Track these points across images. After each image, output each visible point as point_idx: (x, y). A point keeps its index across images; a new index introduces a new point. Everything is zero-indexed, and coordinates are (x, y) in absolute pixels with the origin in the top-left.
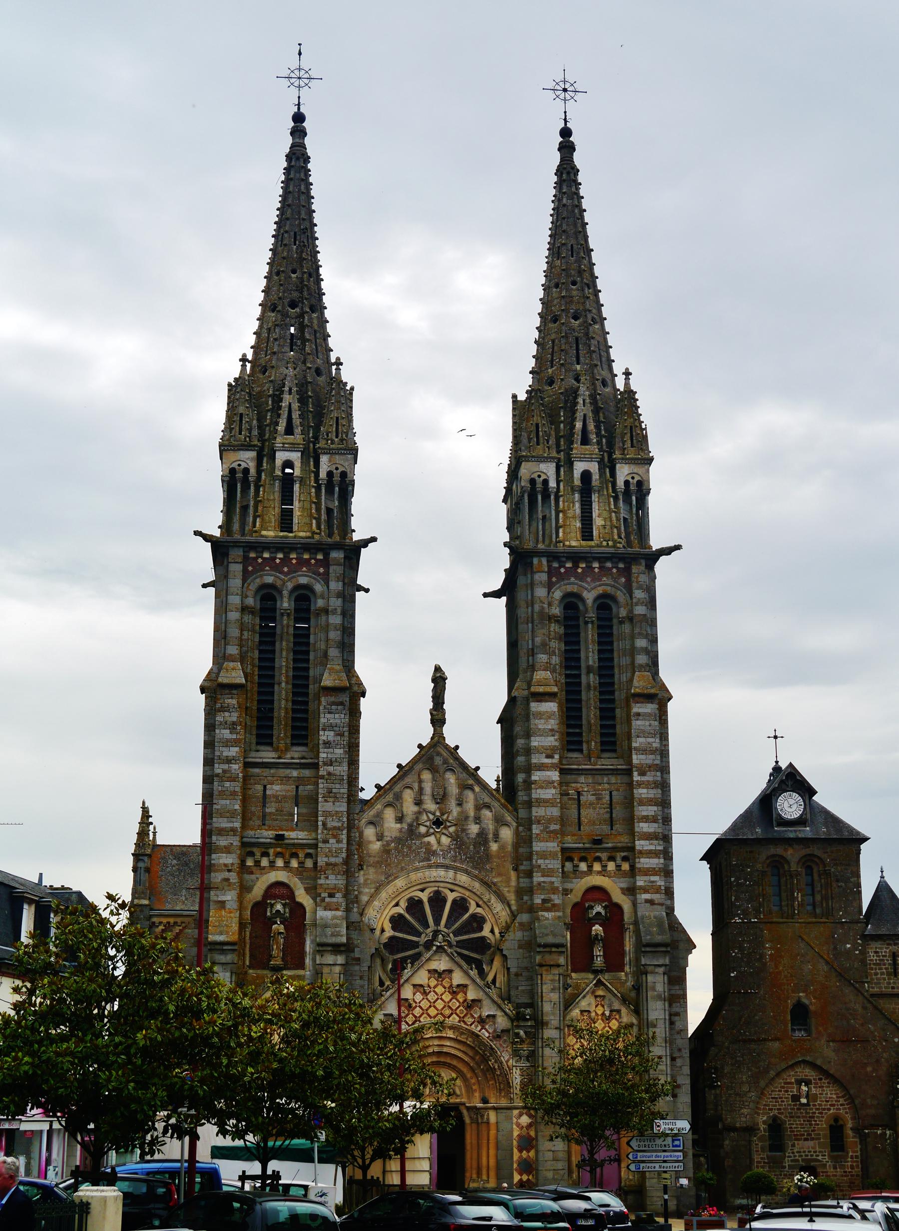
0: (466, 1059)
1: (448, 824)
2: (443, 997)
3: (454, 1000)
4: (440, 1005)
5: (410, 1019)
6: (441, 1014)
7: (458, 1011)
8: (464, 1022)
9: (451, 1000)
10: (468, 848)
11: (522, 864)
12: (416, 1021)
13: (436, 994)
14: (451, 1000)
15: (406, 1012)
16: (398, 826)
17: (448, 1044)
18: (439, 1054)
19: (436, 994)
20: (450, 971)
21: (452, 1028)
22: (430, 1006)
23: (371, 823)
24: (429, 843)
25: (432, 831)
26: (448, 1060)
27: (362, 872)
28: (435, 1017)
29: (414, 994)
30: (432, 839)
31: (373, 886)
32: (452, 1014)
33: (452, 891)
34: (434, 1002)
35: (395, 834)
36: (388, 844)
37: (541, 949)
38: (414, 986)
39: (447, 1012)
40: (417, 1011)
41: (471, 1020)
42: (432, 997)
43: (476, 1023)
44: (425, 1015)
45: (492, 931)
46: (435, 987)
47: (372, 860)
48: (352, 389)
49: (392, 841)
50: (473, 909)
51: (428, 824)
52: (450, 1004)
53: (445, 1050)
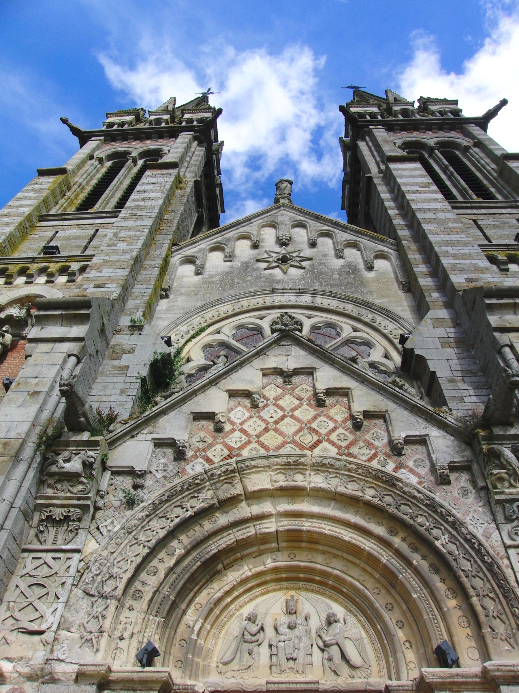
0: (367, 545)
1: (298, 259)
2: (297, 413)
3: (322, 418)
4: (289, 427)
5: (217, 453)
6: (294, 442)
7: (333, 437)
8: (350, 455)
9: (315, 418)
10: (331, 276)
11: (418, 267)
12: (230, 457)
13: (282, 408)
14: (315, 418)
15: (209, 440)
16: (229, 263)
17: (316, 509)
18: (295, 539)
19: (282, 408)
20: (309, 372)
21: (321, 467)
22: (266, 430)
23: (190, 260)
24: (271, 274)
25: (275, 264)
26: (320, 563)
27: (165, 300)
28: (279, 448)
29: (230, 410)
30: (277, 272)
31: (181, 311)
32: (319, 442)
33: (309, 318)
34: (276, 422)
35: (221, 270)
36: (211, 276)
37: (494, 301)
38: (232, 394)
39: (308, 439)
40: (235, 439)
41: (368, 452)
42: (270, 413)
43: (381, 457)
44: (254, 445)
45: (387, 356)
46: (277, 398)
47: (183, 290)
48: (222, 142)
49: (218, 275)
50: (347, 331)
51: (271, 259)
52: (314, 425)
53: (306, 525)
